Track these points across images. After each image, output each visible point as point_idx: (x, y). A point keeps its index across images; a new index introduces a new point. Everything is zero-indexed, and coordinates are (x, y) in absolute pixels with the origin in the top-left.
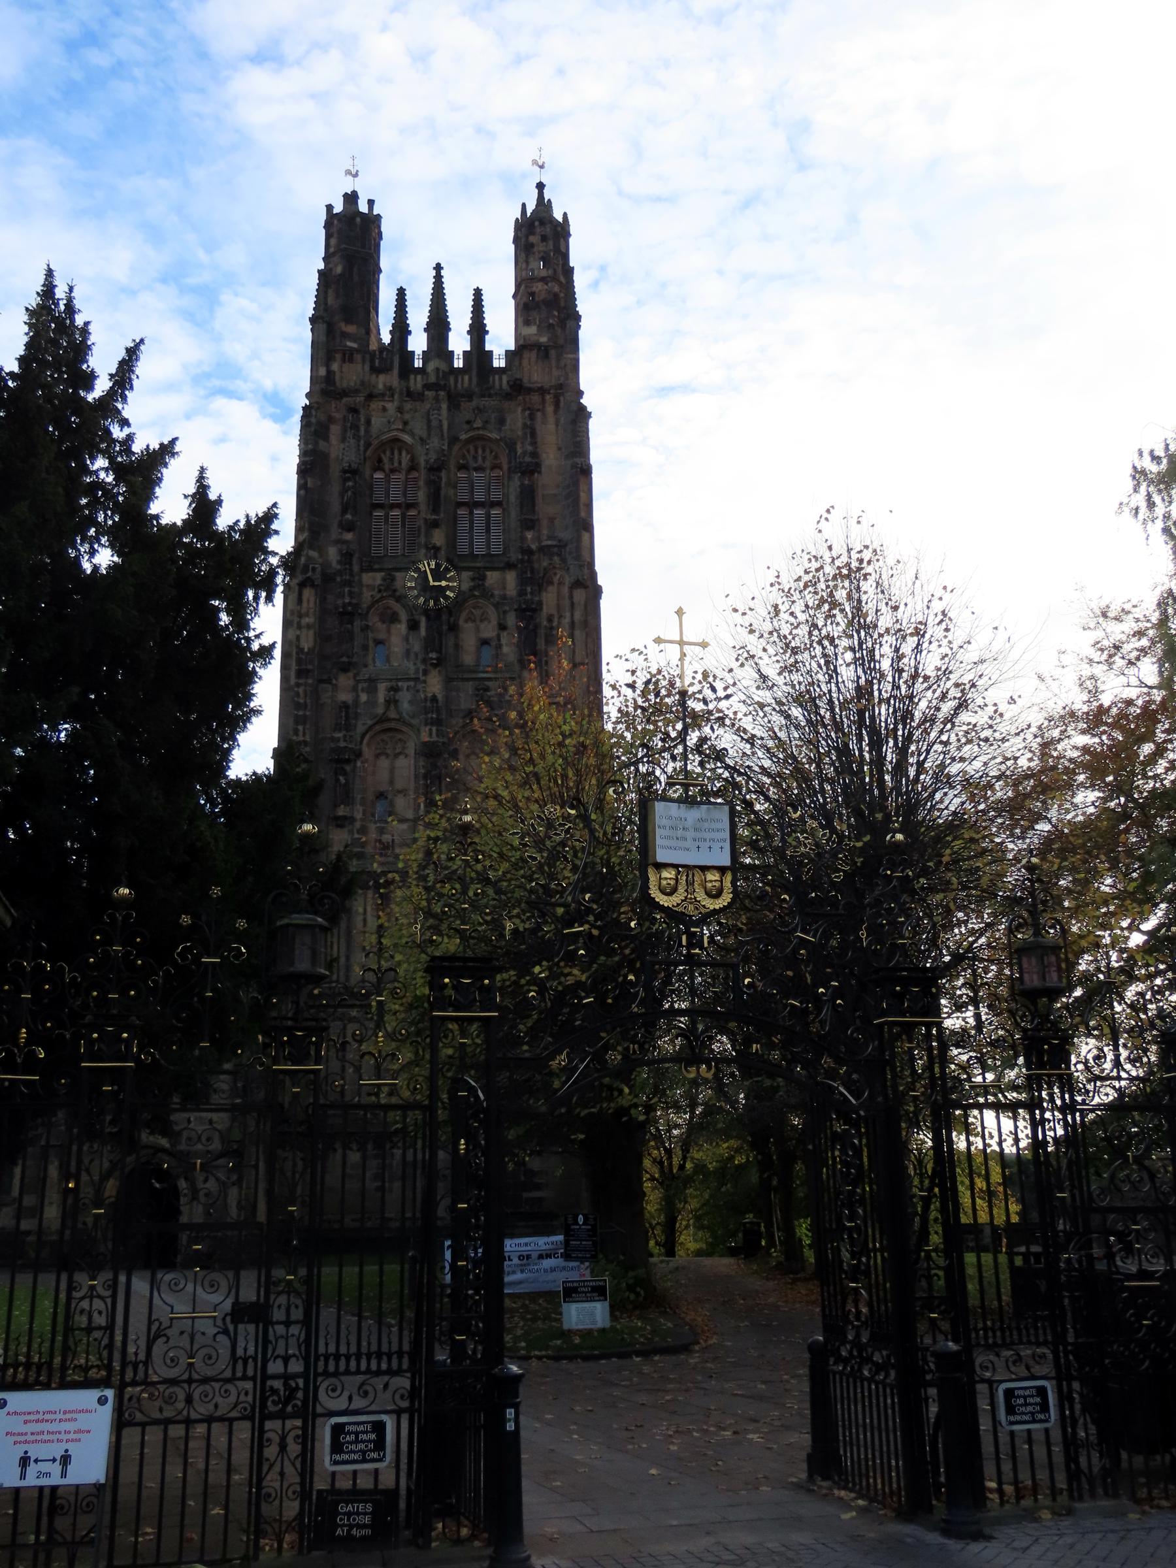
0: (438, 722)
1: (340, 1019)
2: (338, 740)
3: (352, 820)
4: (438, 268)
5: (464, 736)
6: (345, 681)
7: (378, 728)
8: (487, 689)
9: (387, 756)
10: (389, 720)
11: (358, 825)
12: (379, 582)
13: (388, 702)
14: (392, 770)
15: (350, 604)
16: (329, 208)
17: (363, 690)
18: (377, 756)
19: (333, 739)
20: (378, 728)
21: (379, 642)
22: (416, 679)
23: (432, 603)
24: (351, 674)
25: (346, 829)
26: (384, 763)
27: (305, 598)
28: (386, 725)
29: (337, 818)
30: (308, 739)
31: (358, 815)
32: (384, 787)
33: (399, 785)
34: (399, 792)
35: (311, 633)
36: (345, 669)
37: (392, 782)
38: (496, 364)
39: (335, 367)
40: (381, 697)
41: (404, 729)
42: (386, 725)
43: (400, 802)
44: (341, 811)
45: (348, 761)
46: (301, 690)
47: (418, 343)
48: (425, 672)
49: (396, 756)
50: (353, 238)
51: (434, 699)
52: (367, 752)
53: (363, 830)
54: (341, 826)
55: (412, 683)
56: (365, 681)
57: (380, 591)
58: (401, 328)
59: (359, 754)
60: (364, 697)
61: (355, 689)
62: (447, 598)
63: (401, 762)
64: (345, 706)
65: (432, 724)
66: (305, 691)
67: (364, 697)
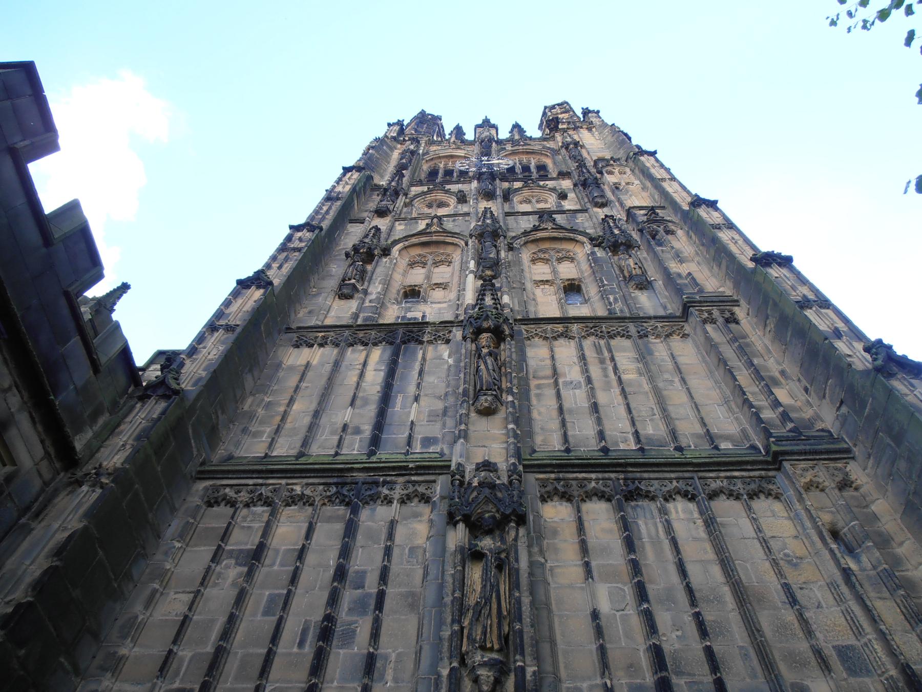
1: (268, 503)
5: (526, 243)
34: (438, 285)
41: (449, 240)
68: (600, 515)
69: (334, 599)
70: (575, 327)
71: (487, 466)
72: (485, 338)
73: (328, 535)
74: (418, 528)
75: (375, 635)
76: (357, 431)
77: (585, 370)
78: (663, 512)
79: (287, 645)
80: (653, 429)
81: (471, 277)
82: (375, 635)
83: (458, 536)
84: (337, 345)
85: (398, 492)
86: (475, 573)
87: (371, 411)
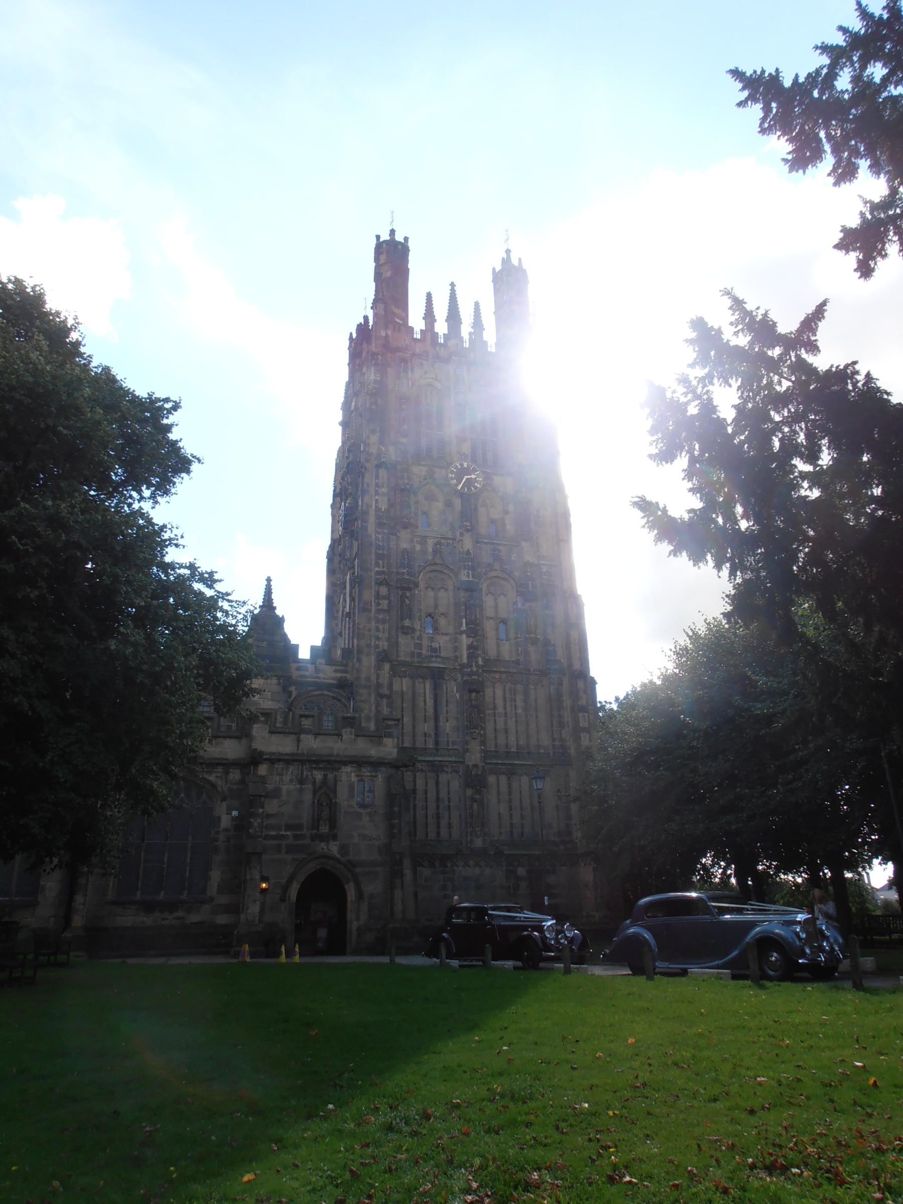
0: (473, 568)
2: (403, 574)
3: (413, 630)
4: (453, 285)
6: (404, 534)
7: (428, 569)
8: (500, 551)
9: (433, 589)
10: (436, 564)
11: (418, 633)
12: (424, 473)
13: (435, 552)
14: (436, 599)
15: (408, 484)
16: (378, 237)
17: (417, 542)
18: (426, 588)
19: (398, 573)
20: (428, 569)
21: (424, 513)
22: (454, 539)
23: (466, 490)
24: (408, 531)
25: (409, 636)
26: (431, 594)
27: (380, 475)
28: (433, 568)
29: (403, 627)
30: (385, 569)
31: (417, 626)
32: (431, 610)
33: (442, 609)
35: (386, 498)
36: (405, 527)
37: (436, 607)
38: (489, 349)
39: (389, 332)
40: (430, 550)
42: (433, 568)
43: (442, 622)
44: (407, 623)
45: (409, 589)
46: (380, 536)
47: (441, 328)
48: (462, 534)
49: (439, 589)
50: (392, 259)
51: (468, 552)
52: (422, 585)
53: (420, 638)
54: (406, 634)
55: (451, 542)
56: (420, 536)
57: (425, 479)
58: (429, 316)
59: (417, 585)
60: (418, 547)
61: (412, 541)
62: (476, 488)
63: (442, 594)
64: (405, 551)
65: (469, 569)
66: (382, 537)
67: (418, 547)
68: (503, 778)
69: (438, 807)
70: (504, 676)
71: (476, 766)
72: (474, 694)
73: (431, 782)
74: (456, 784)
75: (450, 818)
76: (430, 736)
77: (505, 708)
78: (520, 780)
79: (430, 820)
80: (522, 742)
81: (464, 636)
82: (450, 818)
83: (469, 792)
84: (411, 677)
85: (449, 770)
86: (475, 806)
87: (432, 723)
